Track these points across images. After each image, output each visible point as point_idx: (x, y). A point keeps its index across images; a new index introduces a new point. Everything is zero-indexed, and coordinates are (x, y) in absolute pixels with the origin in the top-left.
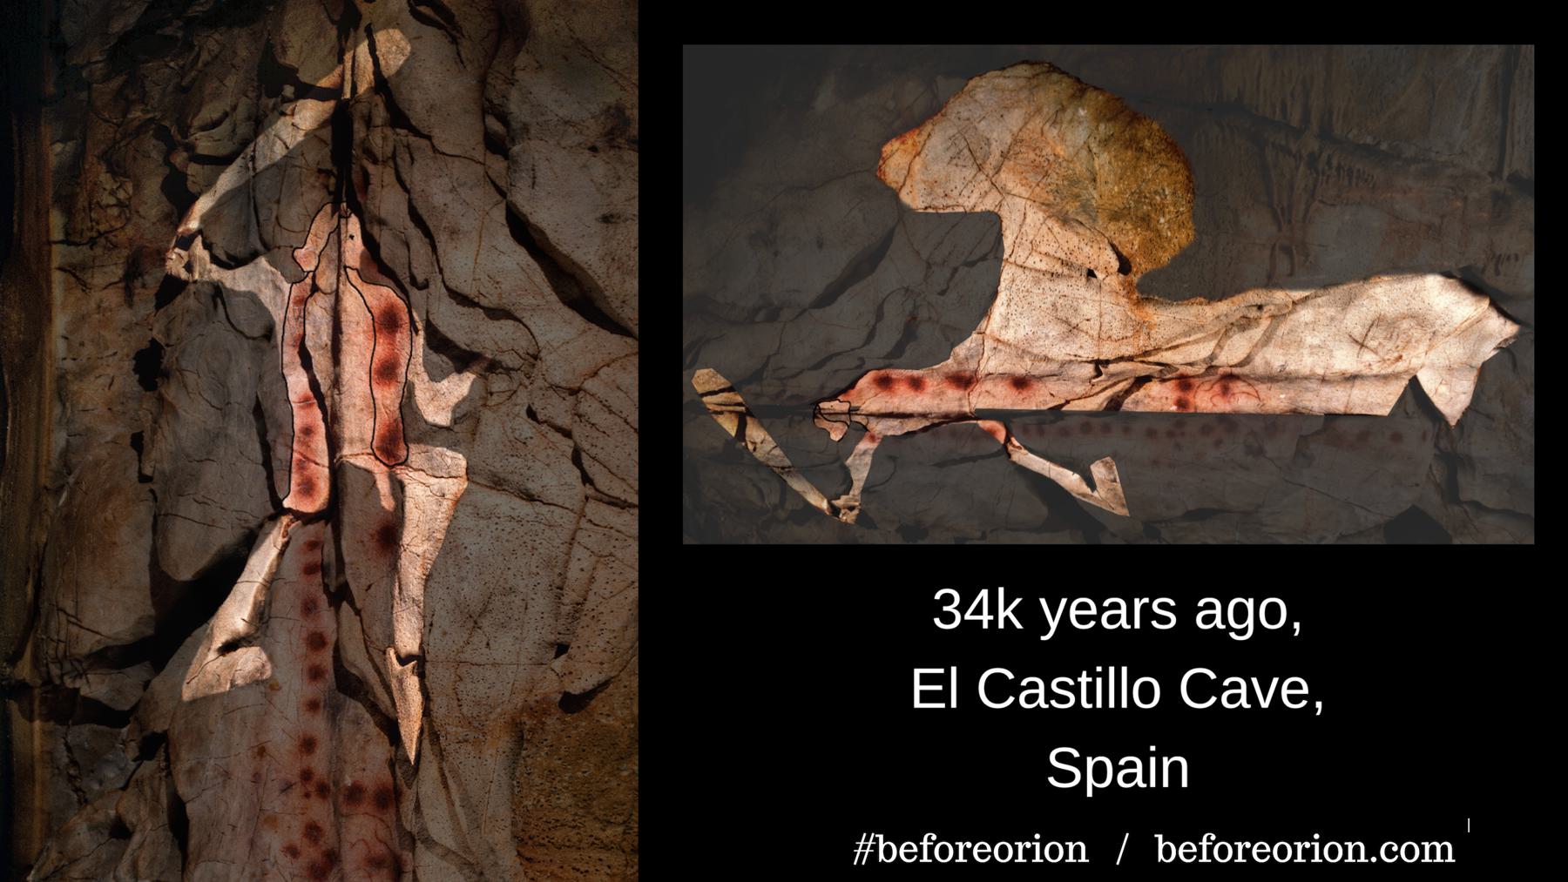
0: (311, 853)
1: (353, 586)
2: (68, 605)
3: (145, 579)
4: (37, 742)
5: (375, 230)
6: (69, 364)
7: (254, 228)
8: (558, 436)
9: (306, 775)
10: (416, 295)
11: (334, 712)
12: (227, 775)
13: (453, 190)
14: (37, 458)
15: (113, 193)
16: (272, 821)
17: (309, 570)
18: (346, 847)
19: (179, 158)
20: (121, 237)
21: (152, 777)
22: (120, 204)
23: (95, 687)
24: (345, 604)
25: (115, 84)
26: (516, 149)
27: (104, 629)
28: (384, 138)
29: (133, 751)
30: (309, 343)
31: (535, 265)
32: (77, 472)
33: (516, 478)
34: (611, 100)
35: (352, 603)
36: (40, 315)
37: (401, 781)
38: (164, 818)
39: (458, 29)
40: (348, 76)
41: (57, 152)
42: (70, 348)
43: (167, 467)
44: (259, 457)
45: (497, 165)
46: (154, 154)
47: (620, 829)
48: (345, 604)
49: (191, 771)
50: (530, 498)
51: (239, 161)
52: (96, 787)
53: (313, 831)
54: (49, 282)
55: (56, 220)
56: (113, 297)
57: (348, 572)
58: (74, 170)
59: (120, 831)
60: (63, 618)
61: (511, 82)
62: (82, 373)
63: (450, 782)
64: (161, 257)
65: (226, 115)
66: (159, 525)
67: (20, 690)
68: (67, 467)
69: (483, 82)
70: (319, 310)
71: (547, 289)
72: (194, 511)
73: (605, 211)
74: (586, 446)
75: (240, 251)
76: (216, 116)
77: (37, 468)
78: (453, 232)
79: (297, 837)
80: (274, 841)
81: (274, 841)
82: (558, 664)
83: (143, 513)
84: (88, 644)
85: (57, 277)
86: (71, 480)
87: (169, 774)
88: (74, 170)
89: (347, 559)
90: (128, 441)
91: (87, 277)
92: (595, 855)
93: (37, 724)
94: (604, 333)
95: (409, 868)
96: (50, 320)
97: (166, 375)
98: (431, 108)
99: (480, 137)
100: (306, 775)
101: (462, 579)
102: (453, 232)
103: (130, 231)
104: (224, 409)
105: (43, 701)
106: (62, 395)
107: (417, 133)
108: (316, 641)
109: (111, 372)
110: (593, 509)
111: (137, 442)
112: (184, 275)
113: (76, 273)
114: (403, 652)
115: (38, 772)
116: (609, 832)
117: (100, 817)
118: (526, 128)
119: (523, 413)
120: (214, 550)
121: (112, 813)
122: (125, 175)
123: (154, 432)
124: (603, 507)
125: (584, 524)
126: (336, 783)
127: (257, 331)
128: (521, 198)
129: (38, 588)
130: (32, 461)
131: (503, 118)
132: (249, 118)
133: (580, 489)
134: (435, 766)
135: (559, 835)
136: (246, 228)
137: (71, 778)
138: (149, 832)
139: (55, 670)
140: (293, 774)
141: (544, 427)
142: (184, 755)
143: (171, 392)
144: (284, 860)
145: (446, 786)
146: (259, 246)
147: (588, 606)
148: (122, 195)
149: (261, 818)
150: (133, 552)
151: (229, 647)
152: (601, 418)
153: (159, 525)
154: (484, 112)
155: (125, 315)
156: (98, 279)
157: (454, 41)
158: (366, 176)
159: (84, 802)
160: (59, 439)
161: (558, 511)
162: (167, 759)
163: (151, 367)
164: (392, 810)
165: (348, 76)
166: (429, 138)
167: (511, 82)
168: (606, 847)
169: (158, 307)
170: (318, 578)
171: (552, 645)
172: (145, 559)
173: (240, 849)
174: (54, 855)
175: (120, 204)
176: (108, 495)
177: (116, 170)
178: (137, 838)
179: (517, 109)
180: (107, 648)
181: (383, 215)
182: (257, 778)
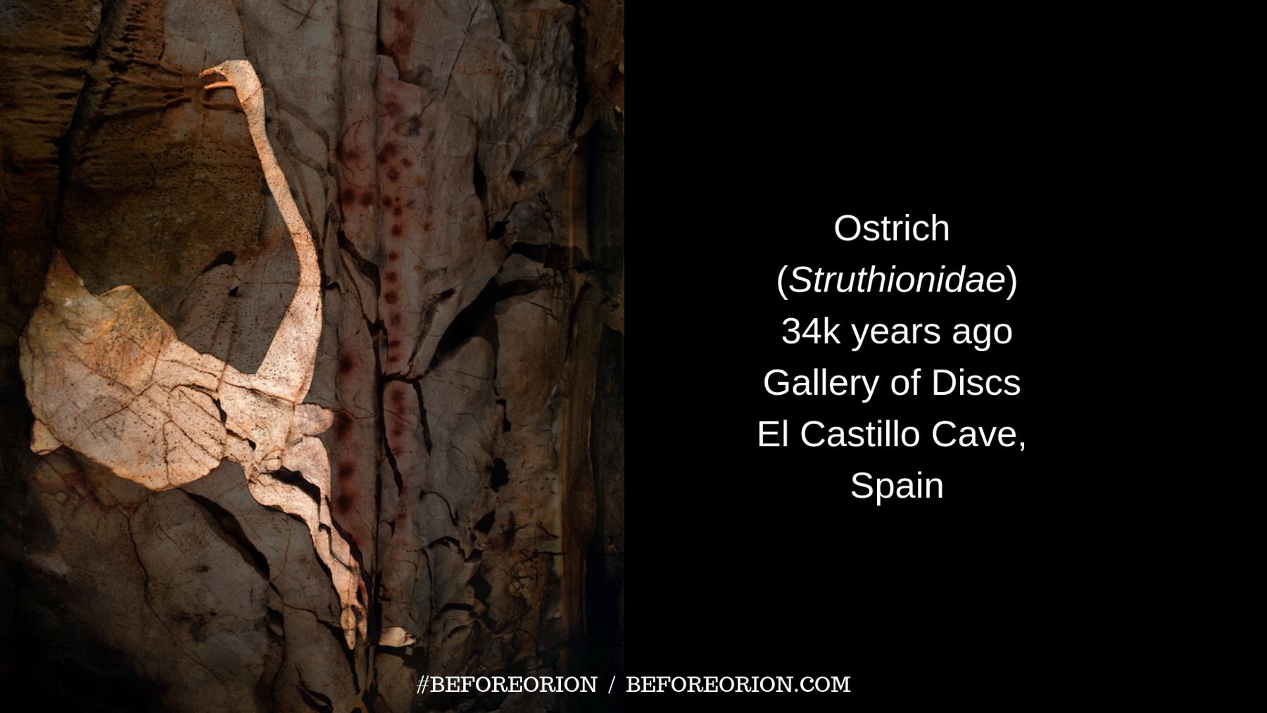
0: (395, 162)
1: (368, 334)
2: (551, 321)
3: (501, 338)
4: (571, 233)
5: (353, 563)
6: (551, 476)
7: (432, 564)
8: (235, 430)
9: (398, 212)
10: (327, 521)
11: (380, 251)
12: (449, 212)
13: (303, 588)
14: (571, 415)
15: (523, 586)
16: (420, 182)
17: (396, 344)
18: (373, 166)
19: (479, 608)
20: (517, 557)
21: (497, 211)
22: (518, 578)
23: (534, 269)
24: (373, 321)
25: (521, 656)
26: (263, 614)
27: (528, 306)
28: (347, 622)
29: (509, 228)
30: (396, 489)
31: (251, 539)
32: (546, 406)
33: (262, 404)
34: (202, 645)
35: (369, 322)
36: (570, 507)
37: (337, 208)
38: (490, 184)
39: (301, 692)
40: (371, 661)
41: (558, 612)
42: (550, 486)
43: (488, 410)
44: (429, 418)
45: (275, 604)
46: (496, 610)
47: (196, 177)
48: (373, 321)
49: (472, 214)
50: (254, 391)
51: (441, 606)
52: (533, 204)
53: (394, 176)
54: (563, 528)
55: (559, 568)
56: (522, 519)
57: (371, 342)
58: (547, 601)
59: (517, 176)
60: (555, 313)
61: (266, 657)
62: (542, 470)
63: (305, 208)
64: (492, 545)
65: (450, 636)
66: (492, 373)
67: (582, 267)
68: (552, 410)
69: (284, 657)
70: (390, 511)
71: (243, 524)
72: (470, 382)
73: (206, 574)
74: (217, 424)
75: (441, 548)
76: (456, 635)
77: (571, 409)
78: (303, 560)
79: (404, 172)
80: (419, 169)
81: (419, 169)
82: (236, 283)
83: (503, 380)
84: (539, 296)
85: (558, 532)
86: (549, 402)
87: (486, 213)
88: (547, 601)
89: (372, 350)
90: (513, 427)
91: (539, 532)
92: (212, 161)
93: (571, 245)
94: (206, 496)
95: (332, 152)
96: (563, 505)
97: (488, 469)
98: (318, 640)
99: (286, 622)
100: (398, 212)
101: (297, 339)
102: (303, 560)
103: (512, 561)
104: (451, 447)
105: (567, 259)
106: (555, 456)
107: (327, 624)
108: (391, 298)
109: (524, 471)
110: (211, 383)
111: (507, 426)
112: (477, 533)
113: (548, 536)
114: (335, 291)
115: (570, 214)
116: (203, 176)
117: (531, 185)
118: (257, 627)
119: (258, 445)
120: (457, 356)
121: (523, 188)
122: (514, 597)
123: (496, 433)
124: (206, 385)
125: (219, 374)
126: (379, 207)
127: (430, 497)
128: (260, 582)
129: (571, 332)
130: (575, 414)
131: (271, 634)
132: (435, 633)
133: (221, 397)
134: (315, 219)
135: (236, 174)
136: (436, 562)
137: (549, 210)
138: (499, 176)
139: (560, 279)
140: (406, 212)
141: (244, 436)
142: (477, 225)
143: (485, 458)
144: (412, 158)
145: (308, 205)
146: (428, 552)
147: (217, 321)
148: (517, 584)
149: (427, 184)
150: (510, 355)
151: (447, 294)
152: (207, 442)
153: (492, 373)
154: (283, 637)
155: (514, 507)
156: (532, 530)
157: (303, 683)
158: (359, 598)
159: (541, 195)
160: (557, 428)
161: (236, 383)
162: (487, 222)
163: (498, 474)
164: (343, 189)
165: (371, 661)
166: (319, 621)
167: (266, 657)
168: (205, 165)
169: (493, 513)
170: (390, 338)
171: (240, 296)
172: (502, 350)
173: (440, 165)
174: (560, 161)
175: (518, 578)
176: (526, 392)
177: (520, 600)
178: (507, 171)
179: (262, 639)
180: (526, 293)
181: (348, 573)
182: (430, 210)
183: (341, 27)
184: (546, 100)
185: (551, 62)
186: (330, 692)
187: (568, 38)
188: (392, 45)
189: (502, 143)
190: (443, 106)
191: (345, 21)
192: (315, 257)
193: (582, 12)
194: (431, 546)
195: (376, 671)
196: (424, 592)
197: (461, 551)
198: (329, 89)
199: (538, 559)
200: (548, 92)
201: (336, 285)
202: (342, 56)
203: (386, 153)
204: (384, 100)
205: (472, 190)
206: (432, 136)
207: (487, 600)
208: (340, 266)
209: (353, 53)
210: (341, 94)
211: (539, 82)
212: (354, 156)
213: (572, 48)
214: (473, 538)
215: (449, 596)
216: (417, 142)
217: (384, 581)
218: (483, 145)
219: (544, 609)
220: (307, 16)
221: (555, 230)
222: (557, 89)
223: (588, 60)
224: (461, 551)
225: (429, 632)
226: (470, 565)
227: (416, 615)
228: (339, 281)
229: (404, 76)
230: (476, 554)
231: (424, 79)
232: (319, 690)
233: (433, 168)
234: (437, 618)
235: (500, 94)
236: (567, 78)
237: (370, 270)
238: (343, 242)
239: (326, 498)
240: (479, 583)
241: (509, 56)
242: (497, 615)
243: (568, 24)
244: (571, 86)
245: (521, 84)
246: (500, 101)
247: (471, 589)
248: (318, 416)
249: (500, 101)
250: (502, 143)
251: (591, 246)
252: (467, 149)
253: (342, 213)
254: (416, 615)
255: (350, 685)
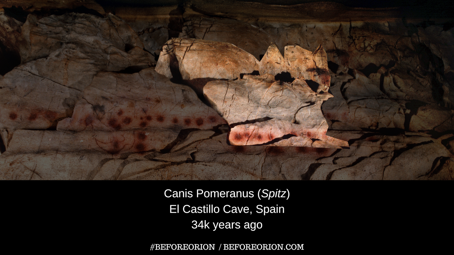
0: (120, 120)
1: (221, 136)
2: (213, 28)
6: (305, 28)
7: (356, 98)
9: (149, 118)
11: (173, 129)
12: (149, 88)
14: (269, 16)
15: (369, 45)
16: (132, 105)
18: (122, 133)
19: (382, 70)
20: (352, 48)
22: (365, 47)
24: (214, 133)
25: (411, 46)
28: (390, 147)
32: (264, 31)
35: (214, 135)
36: (323, 18)
37: (147, 154)
38: (133, 64)
40: (414, 134)
41: (385, 24)
42: (311, 29)
48: (214, 133)
51: (381, 93)
52: (145, 39)
53: (128, 120)
54: (336, 21)
55: (359, 24)
58: (378, 30)
59: (128, 48)
63: (147, 173)
64: (345, 63)
65: (399, 88)
67: (181, 10)
68: (266, 28)
75: (348, 93)
76: (399, 84)
77: (266, 16)
79: (125, 114)
80: (124, 106)
81: (124, 106)
85: (338, 24)
86: (261, 29)
88: (378, 30)
93: (169, 16)
95: (114, 157)
96: (321, 21)
98: (401, 165)
100: (149, 118)
103: (355, 51)
106: (293, 26)
107: (392, 160)
108: (200, 122)
114: (196, 155)
115: (150, 17)
117: (133, 40)
121: (135, 45)
122: (376, 50)
126: (146, 129)
129: (220, 17)
130: (268, 14)
132: (398, 96)
134: (153, 167)
136: (356, 95)
137: (148, 29)
138: (128, 59)
139: (189, 23)
140: (150, 113)
144: (117, 110)
145: (145, 171)
146: (349, 100)
148: (369, 48)
149: (133, 101)
156: (337, 40)
158: (376, 141)
159: (139, 34)
160: (276, 25)
164: (136, 150)
165: (414, 134)
166: (390, 164)
174: (119, 23)
175: (365, 47)
177: (378, 47)
178: (125, 54)
181: (361, 147)
182: (148, 99)
183: (40, 152)
184: (83, 31)
185: (61, 28)
186: (432, 158)
187: (47, 18)
188: (51, 121)
189: (109, 57)
190: (87, 92)
191: (36, 149)
192: (175, 166)
193: (32, 10)
194: (346, 99)
195: (419, 131)
196: (373, 103)
197: (349, 81)
198: (76, 158)
199: (354, 36)
200: (78, 30)
201: (192, 155)
202: (57, 151)
203: (115, 125)
204: (83, 126)
205: (137, 74)
206: (104, 98)
207: (378, 65)
208: (181, 152)
209: (56, 144)
210: (79, 152)
211: (73, 35)
212: (116, 144)
213: (52, 16)
214: (341, 74)
215: (375, 88)
216: (108, 107)
217: (366, 126)
218: (110, 68)
219: (384, 32)
220: (34, 171)
221: (160, 26)
222: (77, 25)
223: (59, 7)
224: (349, 81)
225: (397, 99)
226: (357, 76)
227: (387, 108)
228: (190, 153)
229: (69, 115)
230: (351, 72)
231: (71, 103)
232: (431, 164)
233: (124, 97)
234: (388, 95)
235: (80, 58)
236: (70, 19)
237: (184, 134)
238: (167, 150)
239: (317, 160)
240: (368, 70)
241: (57, 53)
242: (387, 60)
243: (38, 18)
244: (75, 17)
245: (74, 46)
246: (84, 58)
247: (371, 75)
248: (269, 165)
249: (84, 58)
250: (109, 57)
251: (170, 5)
252: (112, 78)
253: (150, 151)
254: (387, 108)
255: (428, 146)
